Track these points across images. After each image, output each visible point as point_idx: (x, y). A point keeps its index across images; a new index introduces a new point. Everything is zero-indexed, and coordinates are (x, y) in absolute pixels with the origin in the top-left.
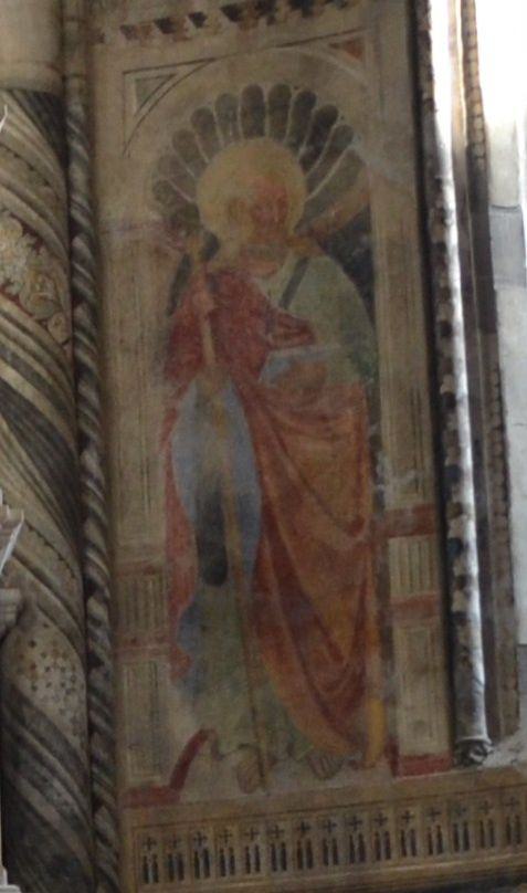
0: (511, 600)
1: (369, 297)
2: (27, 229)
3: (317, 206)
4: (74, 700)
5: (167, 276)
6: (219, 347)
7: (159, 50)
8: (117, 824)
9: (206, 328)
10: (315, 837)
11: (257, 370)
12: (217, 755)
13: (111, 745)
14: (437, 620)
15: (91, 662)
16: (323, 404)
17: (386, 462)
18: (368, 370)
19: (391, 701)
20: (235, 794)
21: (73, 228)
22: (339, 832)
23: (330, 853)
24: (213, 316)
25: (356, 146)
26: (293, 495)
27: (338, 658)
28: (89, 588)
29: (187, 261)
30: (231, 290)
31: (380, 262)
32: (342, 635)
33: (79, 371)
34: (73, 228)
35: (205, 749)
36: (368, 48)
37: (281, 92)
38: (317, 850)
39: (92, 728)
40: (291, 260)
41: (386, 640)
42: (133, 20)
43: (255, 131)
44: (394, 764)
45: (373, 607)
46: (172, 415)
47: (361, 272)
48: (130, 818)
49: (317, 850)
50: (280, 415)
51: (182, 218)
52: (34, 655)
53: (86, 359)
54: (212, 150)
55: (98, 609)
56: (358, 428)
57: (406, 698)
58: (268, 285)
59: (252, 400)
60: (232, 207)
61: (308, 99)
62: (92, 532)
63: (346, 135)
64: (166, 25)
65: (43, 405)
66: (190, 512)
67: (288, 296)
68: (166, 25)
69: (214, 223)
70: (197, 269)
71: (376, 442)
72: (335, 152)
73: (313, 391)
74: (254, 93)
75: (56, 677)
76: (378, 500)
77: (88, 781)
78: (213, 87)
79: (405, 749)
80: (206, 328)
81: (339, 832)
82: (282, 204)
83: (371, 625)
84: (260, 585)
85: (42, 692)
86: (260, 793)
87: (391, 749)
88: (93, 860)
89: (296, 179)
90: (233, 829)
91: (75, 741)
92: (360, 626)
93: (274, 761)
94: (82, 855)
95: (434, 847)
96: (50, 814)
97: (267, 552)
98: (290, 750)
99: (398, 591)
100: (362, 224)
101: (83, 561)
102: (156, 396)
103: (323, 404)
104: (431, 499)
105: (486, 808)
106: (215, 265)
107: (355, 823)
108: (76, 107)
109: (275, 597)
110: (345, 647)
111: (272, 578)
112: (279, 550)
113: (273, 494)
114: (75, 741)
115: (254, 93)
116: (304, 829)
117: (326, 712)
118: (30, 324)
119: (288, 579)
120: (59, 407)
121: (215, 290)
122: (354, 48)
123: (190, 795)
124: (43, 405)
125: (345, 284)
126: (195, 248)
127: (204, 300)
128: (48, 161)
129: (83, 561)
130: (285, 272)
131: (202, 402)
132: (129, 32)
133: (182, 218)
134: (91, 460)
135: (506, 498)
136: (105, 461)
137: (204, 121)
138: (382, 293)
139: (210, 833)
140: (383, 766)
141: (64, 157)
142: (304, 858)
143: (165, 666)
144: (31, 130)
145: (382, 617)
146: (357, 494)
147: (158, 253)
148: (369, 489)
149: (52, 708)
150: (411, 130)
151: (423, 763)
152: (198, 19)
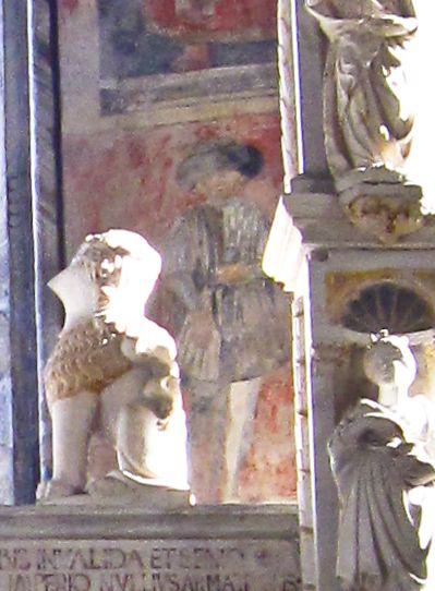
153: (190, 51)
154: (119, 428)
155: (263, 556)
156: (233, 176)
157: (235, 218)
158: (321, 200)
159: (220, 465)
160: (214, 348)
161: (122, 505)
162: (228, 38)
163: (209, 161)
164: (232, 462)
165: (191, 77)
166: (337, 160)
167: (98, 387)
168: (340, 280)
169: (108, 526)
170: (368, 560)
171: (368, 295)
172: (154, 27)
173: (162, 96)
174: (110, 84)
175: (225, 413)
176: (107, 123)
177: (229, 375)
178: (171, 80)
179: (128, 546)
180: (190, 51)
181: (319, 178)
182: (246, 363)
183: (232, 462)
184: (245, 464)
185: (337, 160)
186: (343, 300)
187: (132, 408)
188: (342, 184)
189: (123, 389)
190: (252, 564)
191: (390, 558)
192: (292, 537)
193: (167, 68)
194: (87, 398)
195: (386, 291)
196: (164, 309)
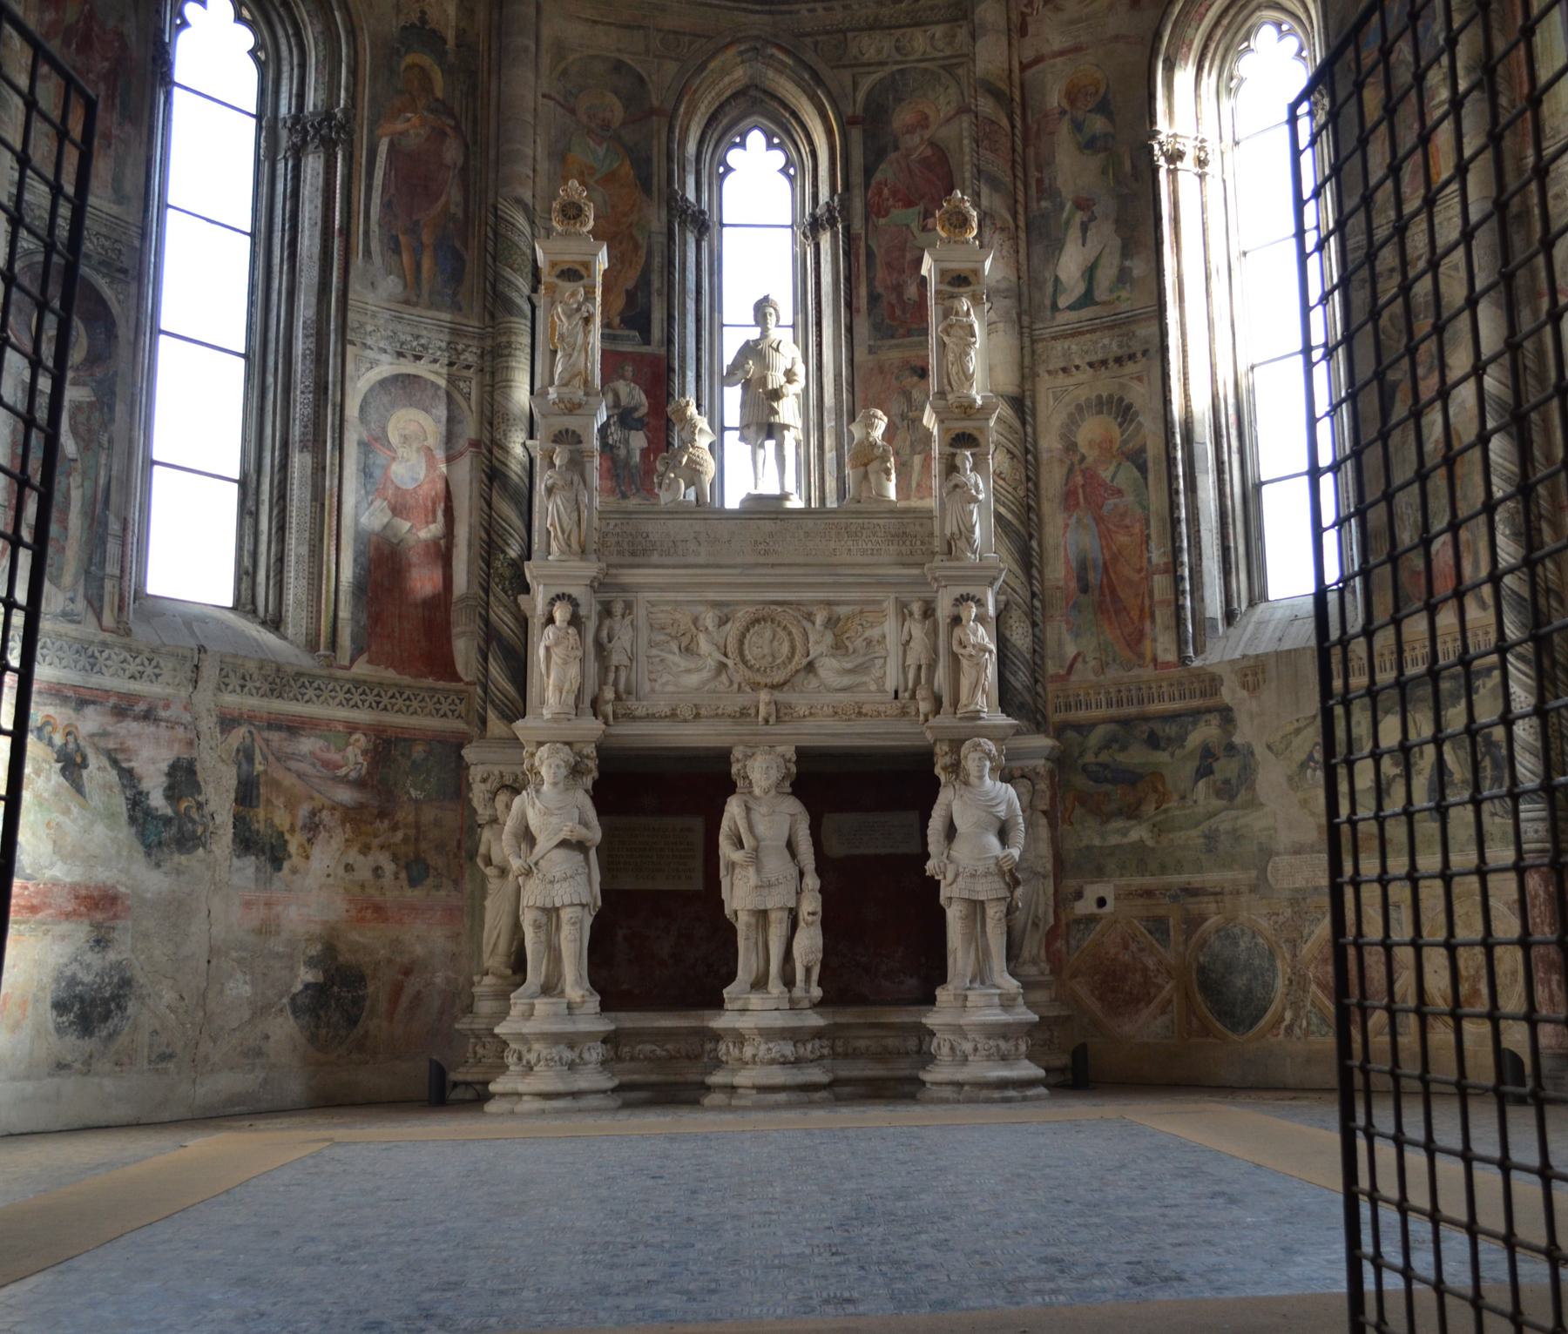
0: (1202, 600)
1: (1146, 479)
2: (1009, 451)
3: (1125, 442)
4: (1028, 640)
5: (1065, 470)
6: (1085, 498)
7: (1061, 380)
8: (1045, 689)
9: (1080, 491)
10: (1124, 694)
11: (1101, 508)
12: (1085, 662)
13: (1042, 658)
14: (1173, 608)
15: (1034, 624)
16: (1127, 521)
17: (1153, 544)
18: (1145, 508)
19: (1154, 640)
20: (1092, 677)
21: (1027, 451)
22: (1133, 692)
23: (1130, 702)
24: (1083, 486)
25: (1141, 418)
26: (1115, 558)
27: (1133, 623)
28: (1034, 595)
29: (1072, 464)
30: (1090, 476)
31: (1150, 465)
32: (1135, 614)
33: (1029, 508)
34: (1027, 451)
35: (1080, 659)
36: (1145, 379)
37: (1111, 397)
38: (1125, 700)
39: (1035, 651)
40: (1114, 464)
41: (1152, 615)
42: (1051, 367)
43: (1100, 412)
44: (1155, 665)
45: (1147, 603)
46: (1067, 526)
47: (1143, 469)
48: (1050, 687)
49: (1125, 700)
50: (1111, 526)
51: (1071, 447)
52: (1011, 622)
53: (1032, 503)
54: (1083, 420)
55: (1037, 603)
56: (1141, 531)
57: (1161, 639)
58: (1105, 474)
59: (1099, 520)
60: (1091, 444)
61: (1121, 399)
62: (1035, 572)
63: (1136, 414)
64: (1064, 370)
65: (1015, 522)
66: (1074, 564)
67: (1112, 481)
68: (1064, 370)
69: (1083, 449)
70: (1077, 467)
71: (1148, 536)
72: (1132, 421)
73: (1123, 516)
74: (1099, 397)
75: (1020, 631)
76: (1149, 560)
77: (1033, 672)
78: (1083, 394)
79: (1160, 660)
80: (1080, 491)
81: (1133, 692)
82: (1111, 441)
83: (1147, 609)
84: (1102, 594)
85: (1015, 636)
86: (1102, 677)
87: (1155, 660)
88: (1035, 703)
89: (1116, 431)
90: (1091, 692)
91: (1028, 656)
92: (1142, 610)
93: (1108, 664)
94: (1031, 702)
95: (1172, 699)
96: (1018, 685)
97: (1105, 580)
98: (1114, 660)
99: (1157, 596)
100: (1143, 450)
101: (1031, 584)
102: (1060, 519)
103: (1127, 521)
104: (1170, 559)
105: (1192, 683)
106: (1083, 466)
107: (1140, 689)
108: (1028, 403)
109: (1108, 599)
110: (1136, 618)
111: (1107, 592)
112: (1109, 578)
113: (1107, 557)
114: (1028, 656)
115: (1099, 397)
116: (1119, 691)
117: (1129, 645)
118: (1010, 490)
119: (1113, 591)
120: (1022, 522)
121: (1084, 476)
122: (1140, 379)
123: (1074, 678)
124: (1015, 522)
125: (1137, 474)
126: (1076, 459)
127: (1080, 480)
128: (1017, 424)
129: (1031, 584)
130: (1112, 469)
131: (1079, 521)
132: (1049, 372)
133: (1071, 447)
134: (1034, 544)
135: (1201, 559)
136: (1040, 544)
137: (1079, 408)
138: (1151, 477)
139: (1082, 693)
140: (1151, 666)
141: (1024, 423)
142: (1120, 703)
143: (1064, 626)
144: (1010, 412)
145: (1151, 607)
146: (1141, 557)
147: (1061, 461)
148: (1146, 555)
149: (1019, 643)
150: (1162, 412)
151: (1167, 665)
152: (1077, 367)
153: (901, 331)
154: (872, 478)
155: (921, 525)
156: (915, 379)
157: (915, 394)
158: (943, 402)
159: (909, 484)
160: (908, 443)
161: (874, 507)
162: (915, 326)
163: (907, 373)
164: (914, 484)
165: (900, 341)
166: (947, 388)
167: (866, 465)
168: (948, 430)
169: (871, 514)
170: (955, 530)
171: (957, 435)
172: (887, 321)
173: (891, 347)
174: (871, 343)
175: (912, 467)
176: (871, 357)
177: (913, 452)
178: (893, 342)
179: (875, 521)
180: (901, 331)
181: (941, 394)
182: (919, 449)
183: (914, 484)
184: (918, 485)
185: (947, 388)
186: (948, 438)
187: (877, 473)
188: (950, 397)
189: (872, 467)
190: (918, 528)
191: (963, 528)
192: (931, 518)
193: (892, 337)
194: (862, 469)
195: (964, 434)
196: (889, 434)
